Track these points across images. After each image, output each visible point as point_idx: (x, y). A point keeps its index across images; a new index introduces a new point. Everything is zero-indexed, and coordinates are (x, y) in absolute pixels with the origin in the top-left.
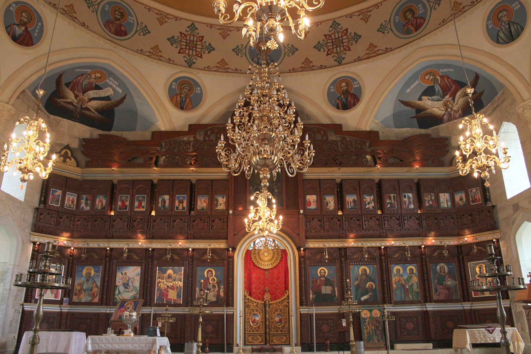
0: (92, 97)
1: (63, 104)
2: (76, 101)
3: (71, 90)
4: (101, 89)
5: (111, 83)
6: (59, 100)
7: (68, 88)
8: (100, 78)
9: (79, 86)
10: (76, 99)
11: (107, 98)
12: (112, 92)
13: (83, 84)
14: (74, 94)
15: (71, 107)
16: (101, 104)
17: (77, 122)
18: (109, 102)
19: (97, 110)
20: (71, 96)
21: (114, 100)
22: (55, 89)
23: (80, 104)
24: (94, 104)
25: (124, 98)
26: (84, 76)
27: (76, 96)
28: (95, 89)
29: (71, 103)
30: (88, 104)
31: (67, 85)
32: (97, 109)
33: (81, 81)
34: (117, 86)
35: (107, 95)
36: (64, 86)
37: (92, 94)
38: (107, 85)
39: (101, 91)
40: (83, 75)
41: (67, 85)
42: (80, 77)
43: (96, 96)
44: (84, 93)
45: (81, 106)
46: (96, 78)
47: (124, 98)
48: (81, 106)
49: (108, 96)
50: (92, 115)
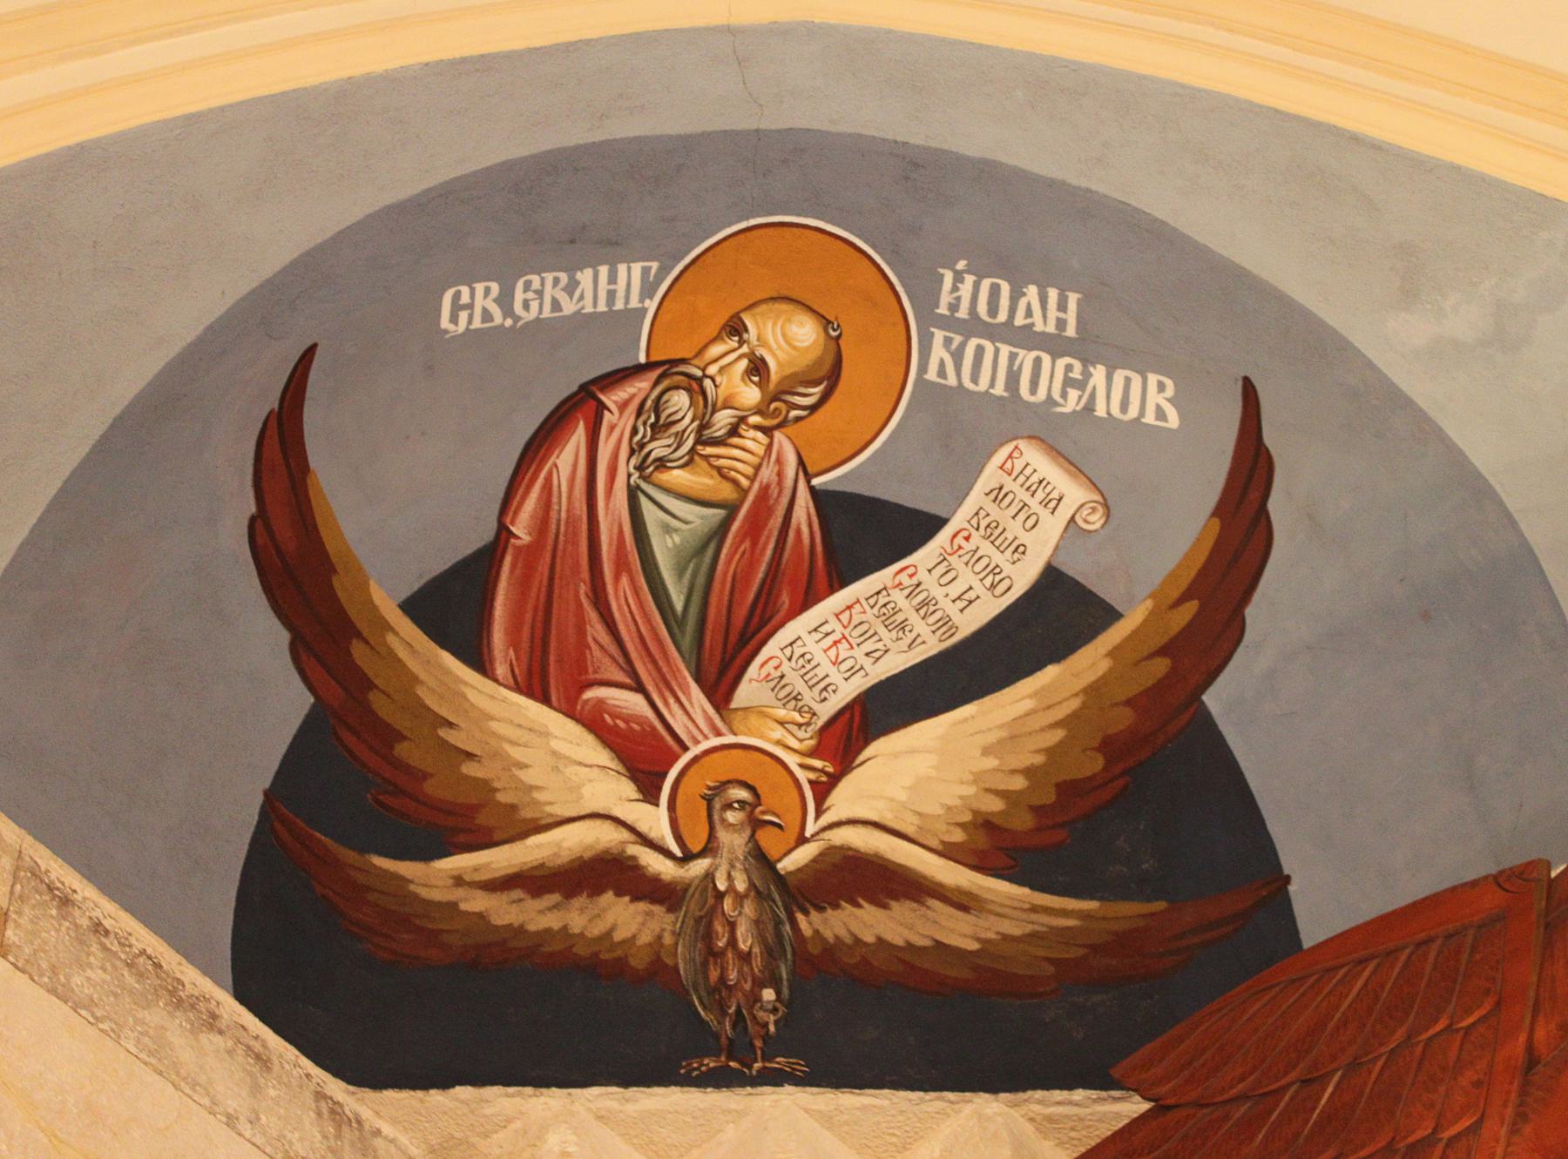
0: (847, 690)
1: (505, 911)
2: (655, 820)
3: (534, 686)
4: (921, 527)
5: (988, 370)
6: (436, 877)
7: (480, 662)
8: (830, 374)
9: (623, 595)
10: (649, 793)
11: (1053, 615)
12: (1074, 494)
13: (663, 549)
14: (596, 723)
15: (622, 920)
16: (1014, 736)
17: (774, 1079)
18: (1090, 661)
19: (993, 845)
20: (558, 771)
21: (1143, 577)
22: (291, 702)
23: (733, 841)
24: (919, 783)
25: (1252, 468)
26: (618, 423)
27: (645, 760)
28: (840, 578)
29: (606, 873)
30: (842, 802)
31: (452, 610)
32: (985, 824)
33: (613, 511)
34: (1086, 347)
35: (1023, 576)
36: (410, 642)
37: (829, 648)
38: (967, 430)
39: (923, 557)
40: (583, 403)
41: (452, 610)
42: (567, 457)
43: (897, 662)
44: (720, 685)
45: (761, 859)
46: (777, 407)
47: (1252, 468)
48: (761, 859)
49: (1052, 577)
50: (960, 932)
